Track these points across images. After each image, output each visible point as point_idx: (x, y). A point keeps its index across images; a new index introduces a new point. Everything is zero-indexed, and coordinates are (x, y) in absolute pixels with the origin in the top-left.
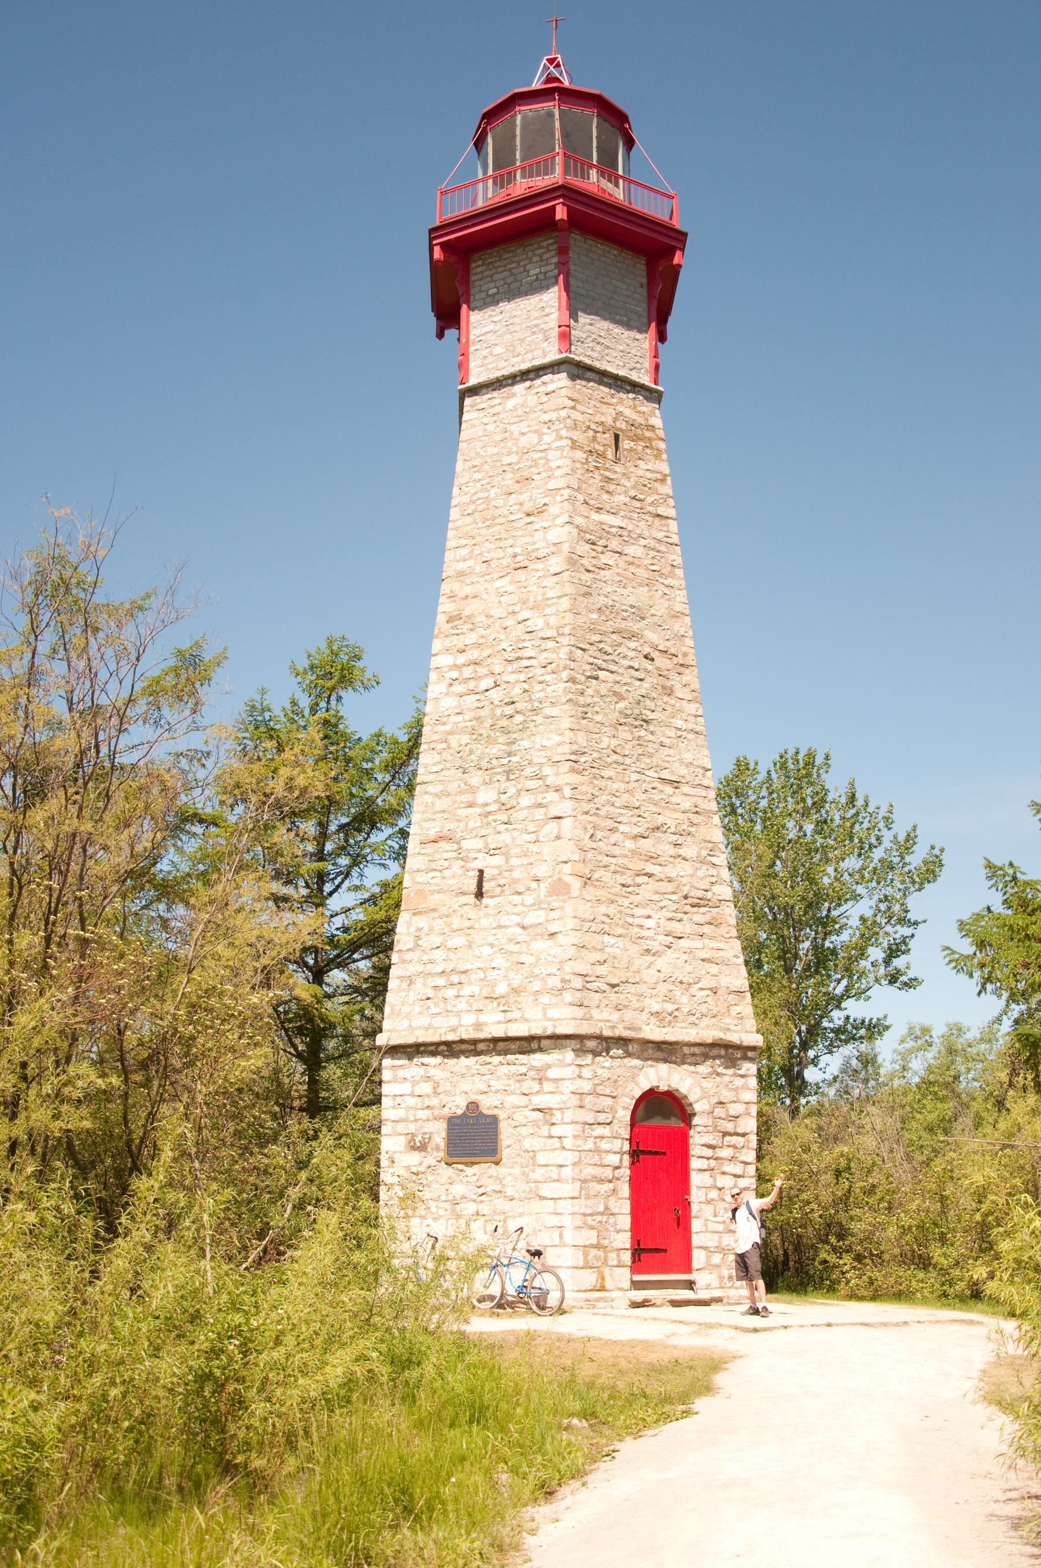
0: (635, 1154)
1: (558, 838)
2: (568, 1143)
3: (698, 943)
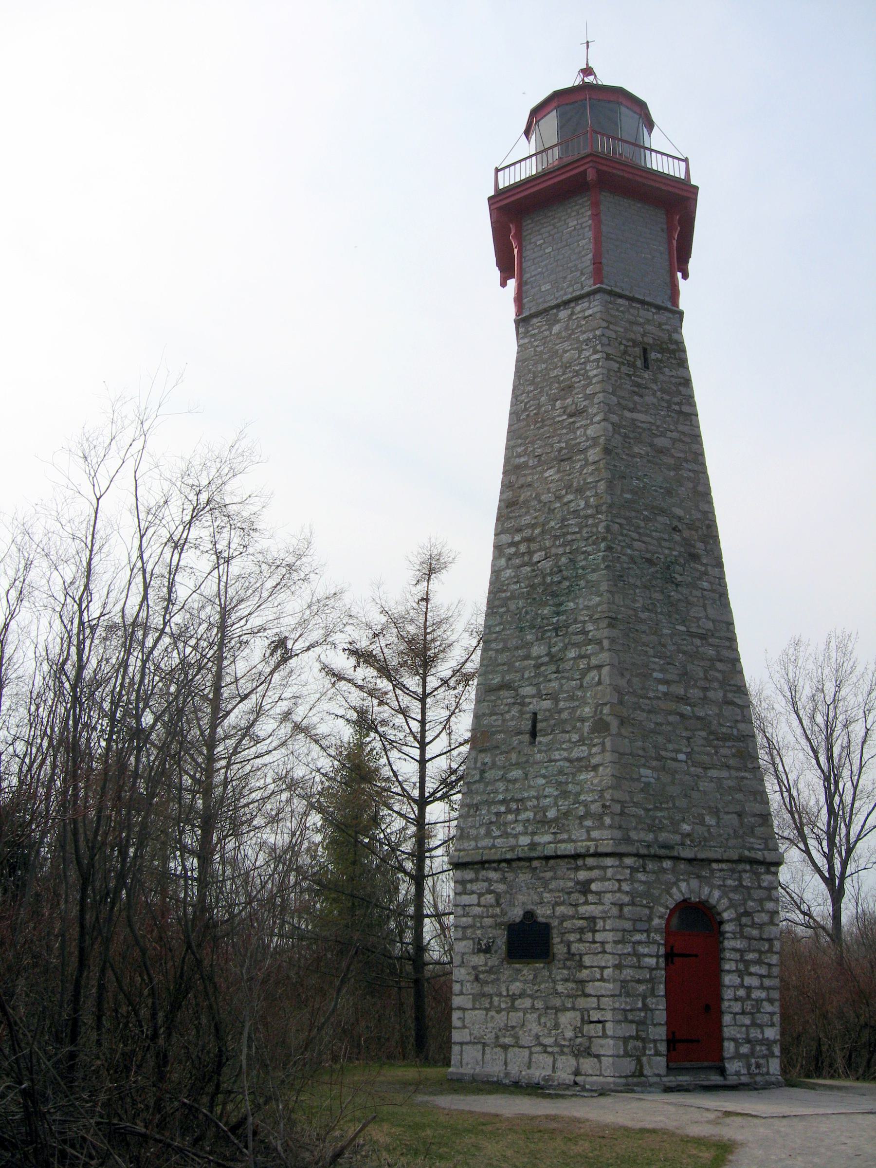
0: (670, 956)
1: (599, 683)
2: (609, 948)
3: (724, 774)
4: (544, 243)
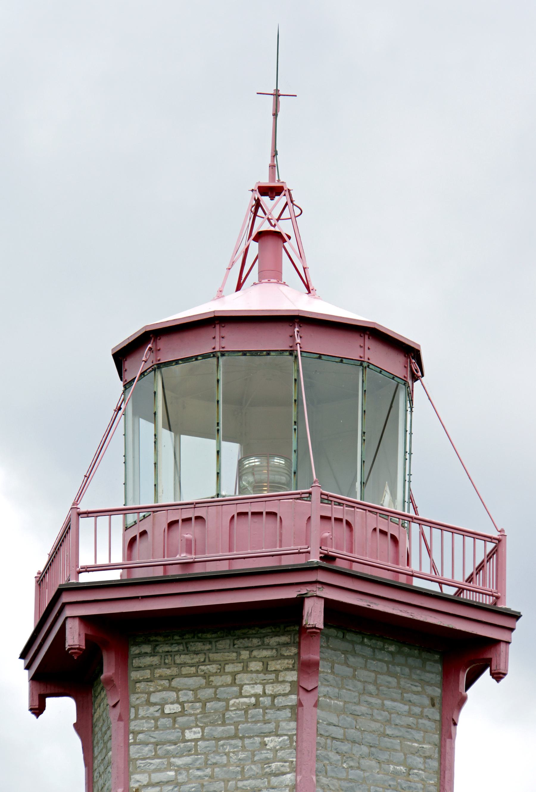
4: (183, 713)
